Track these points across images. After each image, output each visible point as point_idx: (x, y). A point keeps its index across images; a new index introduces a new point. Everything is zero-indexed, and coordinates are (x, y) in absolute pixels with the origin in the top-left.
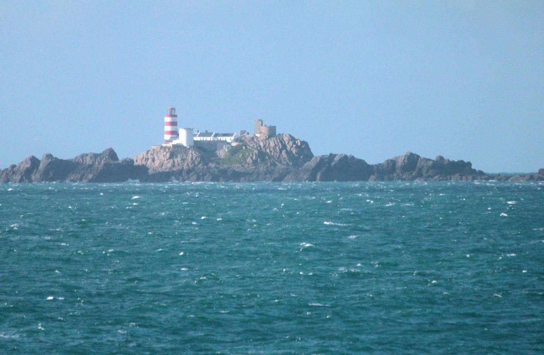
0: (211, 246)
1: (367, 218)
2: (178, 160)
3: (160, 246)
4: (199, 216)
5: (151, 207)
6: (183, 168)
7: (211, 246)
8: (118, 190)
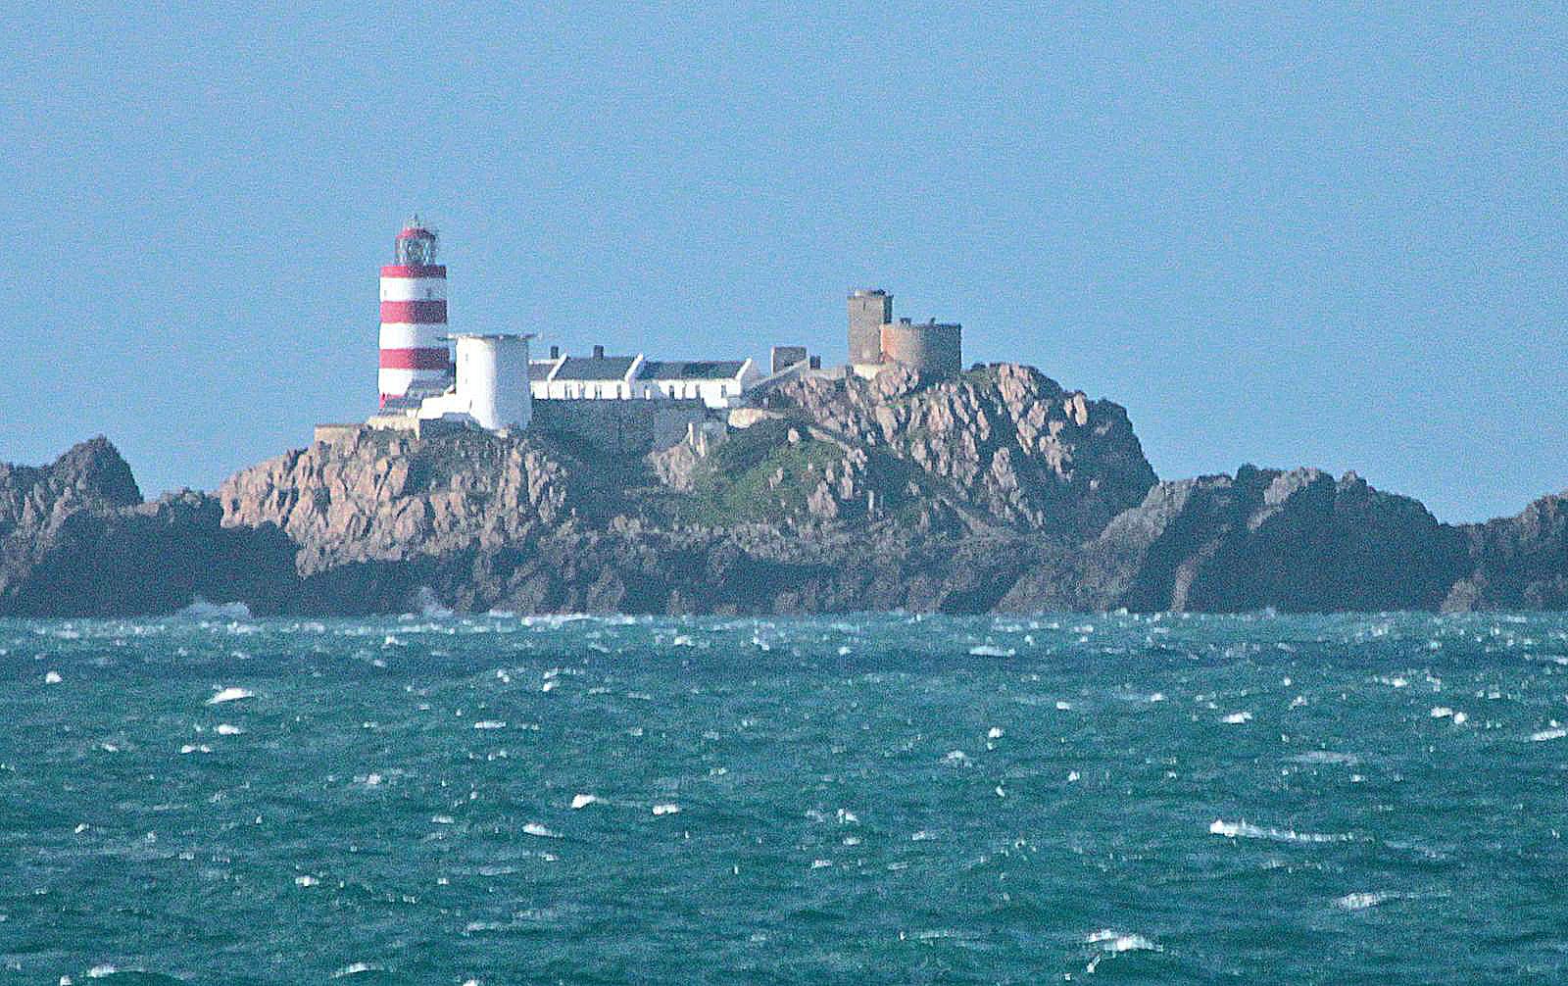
0: (623, 948)
1: (1437, 803)
2: (450, 499)
3: (356, 946)
4: (557, 791)
5: (313, 745)
6: (476, 541)
7: (623, 948)
8: (136, 659)
